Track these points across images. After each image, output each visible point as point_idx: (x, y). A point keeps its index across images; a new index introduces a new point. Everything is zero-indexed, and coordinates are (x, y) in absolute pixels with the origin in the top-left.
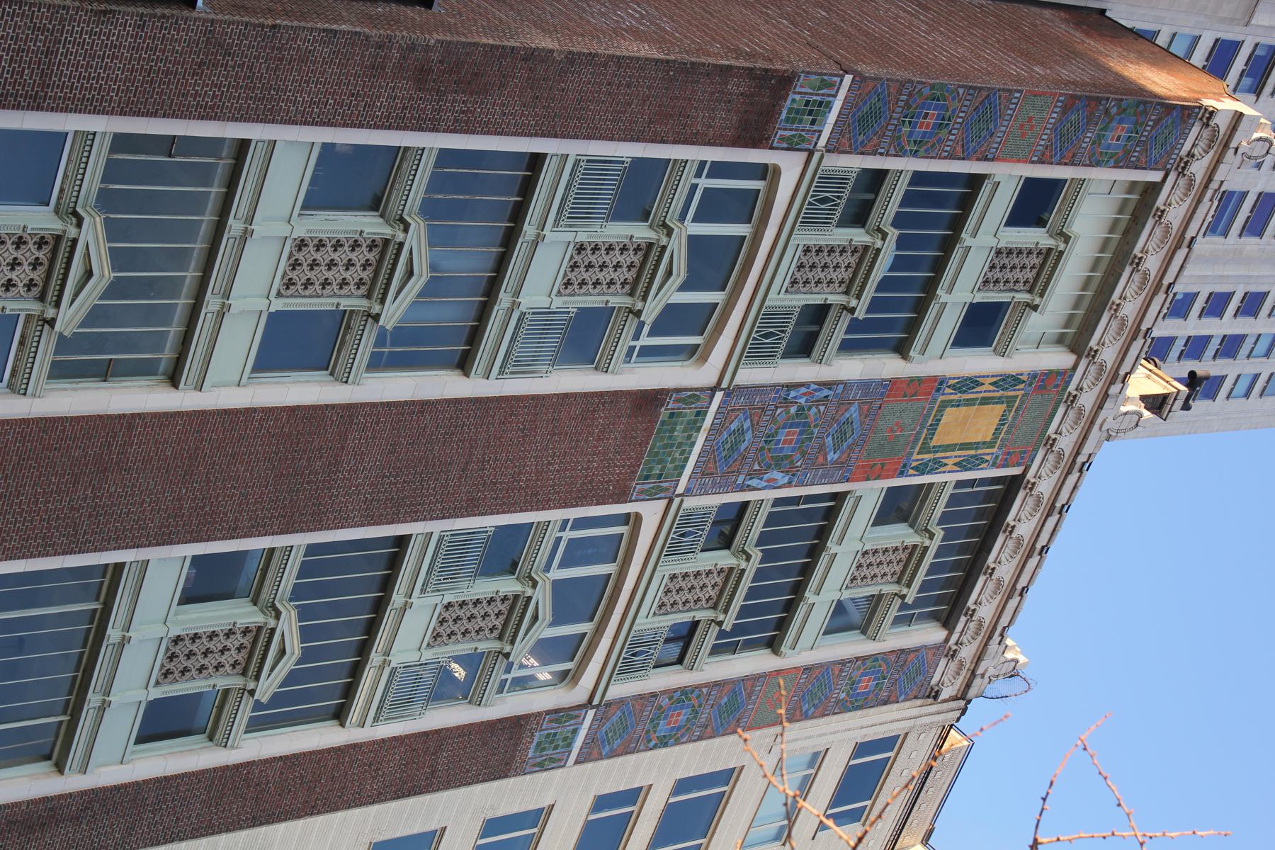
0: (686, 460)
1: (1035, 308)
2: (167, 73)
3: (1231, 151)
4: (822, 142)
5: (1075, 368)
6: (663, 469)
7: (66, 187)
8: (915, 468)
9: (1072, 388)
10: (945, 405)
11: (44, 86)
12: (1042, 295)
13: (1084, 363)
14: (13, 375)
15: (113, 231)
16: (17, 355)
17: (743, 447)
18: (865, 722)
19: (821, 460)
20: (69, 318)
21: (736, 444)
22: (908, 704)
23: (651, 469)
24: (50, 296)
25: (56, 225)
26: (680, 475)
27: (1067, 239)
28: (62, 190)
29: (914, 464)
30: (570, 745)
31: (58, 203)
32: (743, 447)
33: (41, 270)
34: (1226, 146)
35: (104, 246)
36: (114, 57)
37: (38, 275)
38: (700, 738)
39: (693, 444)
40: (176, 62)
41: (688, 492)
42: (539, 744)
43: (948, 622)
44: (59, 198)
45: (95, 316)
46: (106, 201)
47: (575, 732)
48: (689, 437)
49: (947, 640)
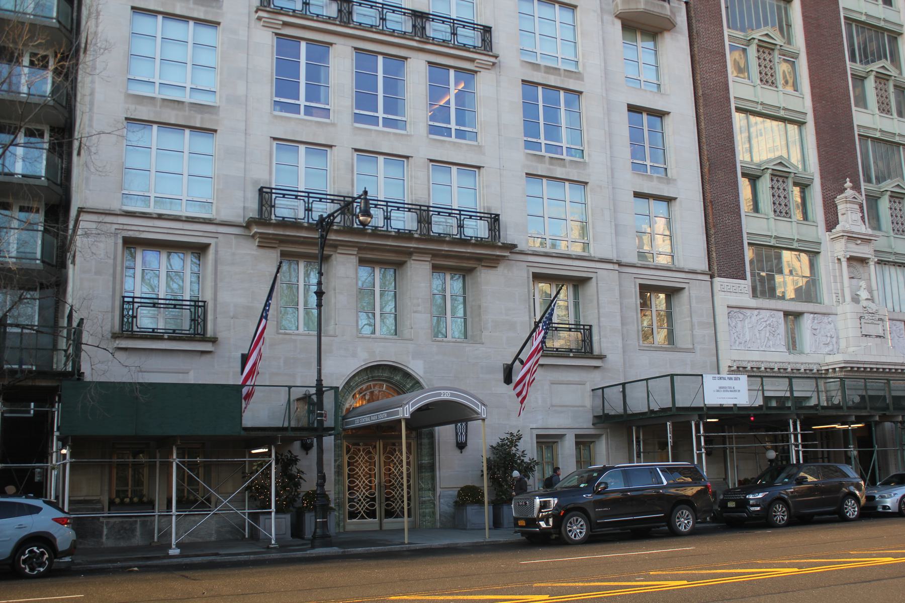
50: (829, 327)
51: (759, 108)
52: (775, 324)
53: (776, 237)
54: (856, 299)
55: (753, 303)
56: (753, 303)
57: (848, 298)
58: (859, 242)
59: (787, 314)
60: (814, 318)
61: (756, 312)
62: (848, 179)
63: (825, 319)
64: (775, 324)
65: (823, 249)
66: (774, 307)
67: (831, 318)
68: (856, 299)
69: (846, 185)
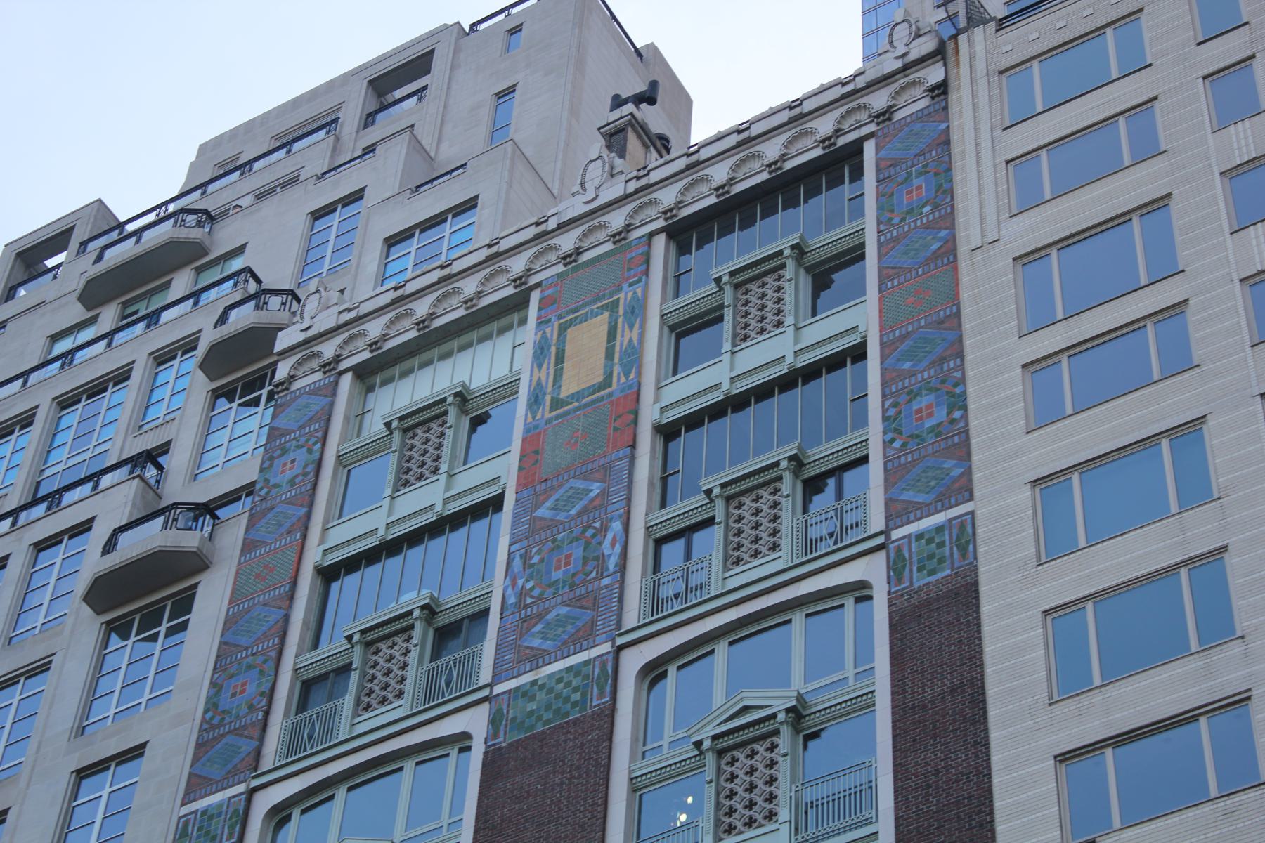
0: (569, 669)
1: (462, 397)
3: (310, 333)
4: (241, 788)
5: (538, 285)
6: (575, 690)
8: (627, 375)
9: (560, 268)
10: (557, 403)
12: (444, 400)
13: (533, 280)
17: (564, 610)
18: (970, 148)
19: (596, 503)
21: (560, 622)
22: (954, 110)
23: (575, 704)
26: (587, 663)
27: (388, 425)
29: (623, 380)
30: (939, 529)
32: (564, 610)
34: (307, 342)
38: (960, 355)
39: (551, 676)
41: (497, 678)
42: (932, 572)
43: (855, 150)
47: (919, 536)
48: (542, 687)
49: (871, 135)
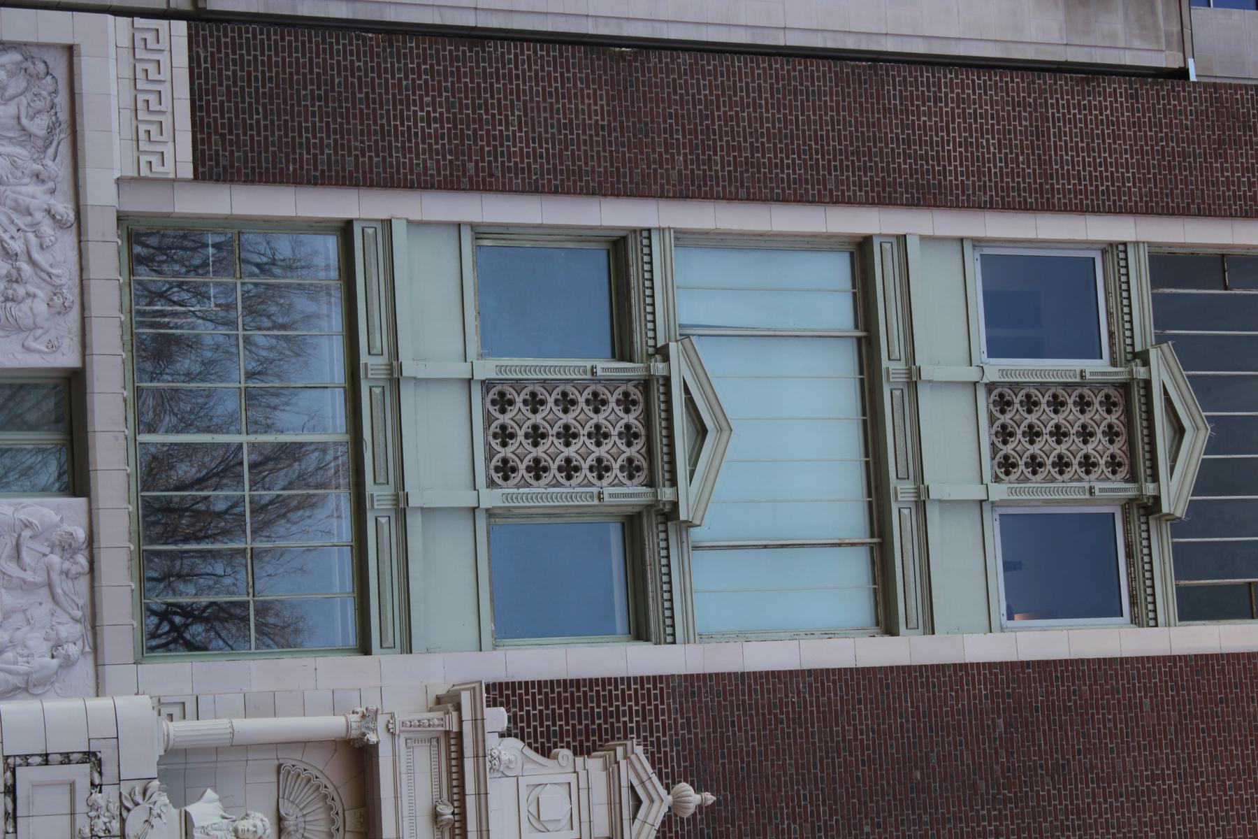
2: (1184, 155)
7: (1114, 328)
11: (1047, 176)
14: (1133, 603)
15: (1188, 354)
16: (1129, 574)
20: (1175, 491)
24: (1142, 470)
25: (1120, 373)
28: (1111, 335)
31: (1112, 353)
33: (1120, 442)
35: (1182, 375)
36: (1116, 138)
37: (1117, 448)
40: (1190, 141)
44: (1112, 345)
45: (1208, 478)
46: (1165, 315)
50: (37, 642)
51: (892, 367)
52: (21, 312)
53: (394, 380)
54: (184, 768)
55: (102, 194)
56: (102, 194)
57: (184, 729)
58: (447, 811)
59: (71, 388)
60: (66, 547)
61: (64, 208)
62: (710, 798)
63: (70, 630)
64: (21, 312)
65: (384, 662)
66: (95, 309)
67: (85, 668)
68: (184, 768)
69: (685, 787)
